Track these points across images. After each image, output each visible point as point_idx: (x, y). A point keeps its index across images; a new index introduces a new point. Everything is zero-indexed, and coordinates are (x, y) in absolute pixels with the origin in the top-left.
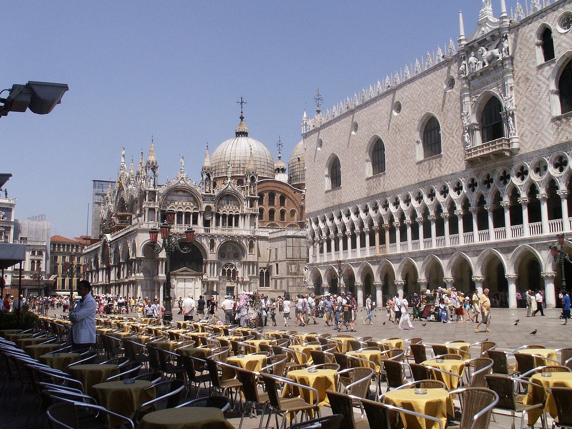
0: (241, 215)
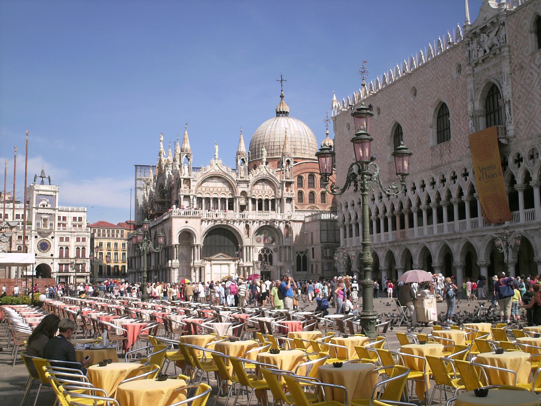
0: (278, 199)
